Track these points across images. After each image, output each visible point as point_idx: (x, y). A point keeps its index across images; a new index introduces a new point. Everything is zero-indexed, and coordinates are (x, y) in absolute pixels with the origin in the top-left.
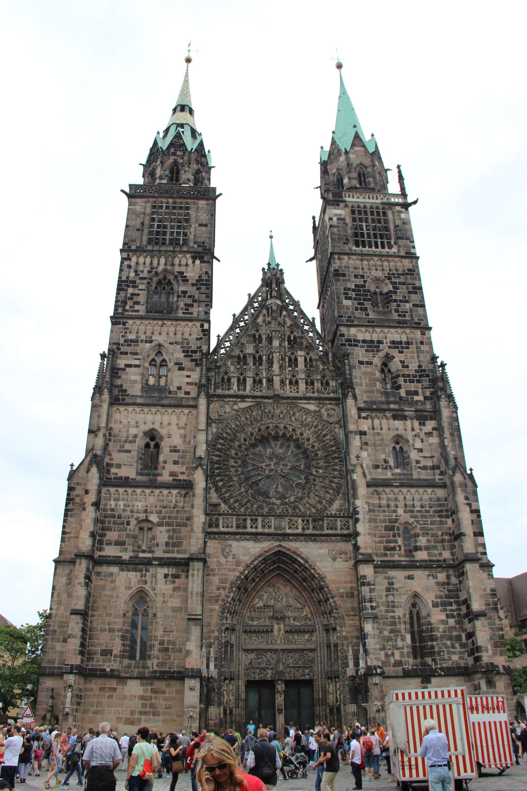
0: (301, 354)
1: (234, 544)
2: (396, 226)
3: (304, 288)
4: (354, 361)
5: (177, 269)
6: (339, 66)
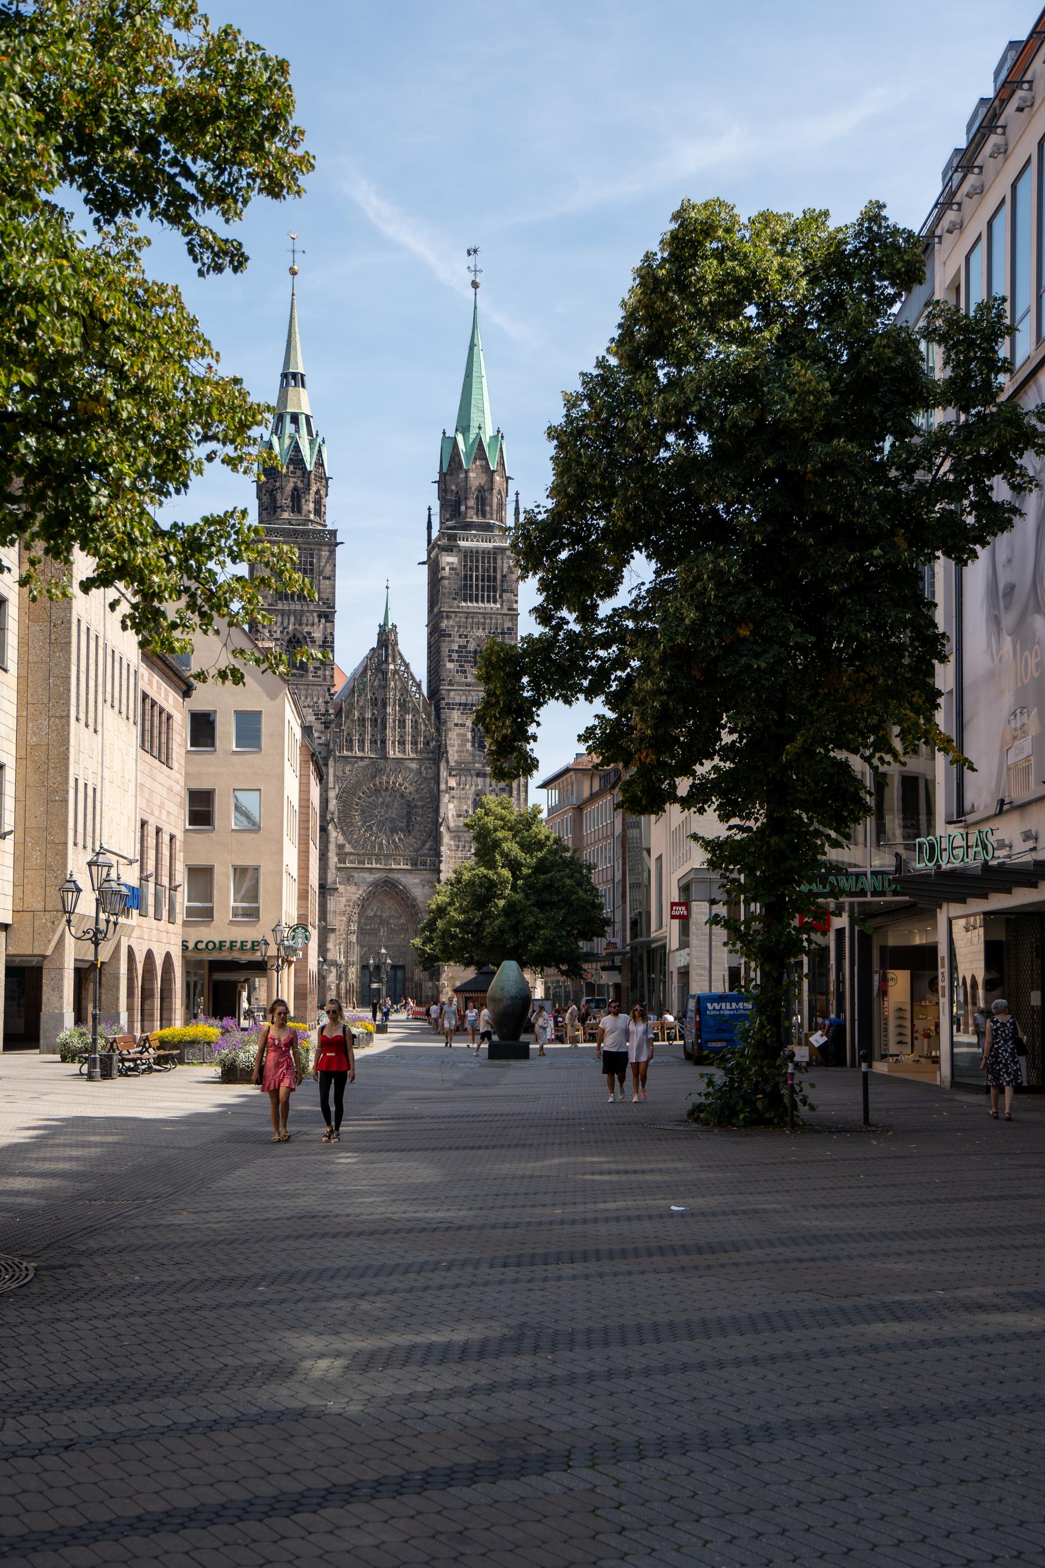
0: (409, 717)
1: (356, 875)
2: (504, 576)
3: (414, 649)
4: (450, 725)
5: (306, 629)
6: (475, 285)
